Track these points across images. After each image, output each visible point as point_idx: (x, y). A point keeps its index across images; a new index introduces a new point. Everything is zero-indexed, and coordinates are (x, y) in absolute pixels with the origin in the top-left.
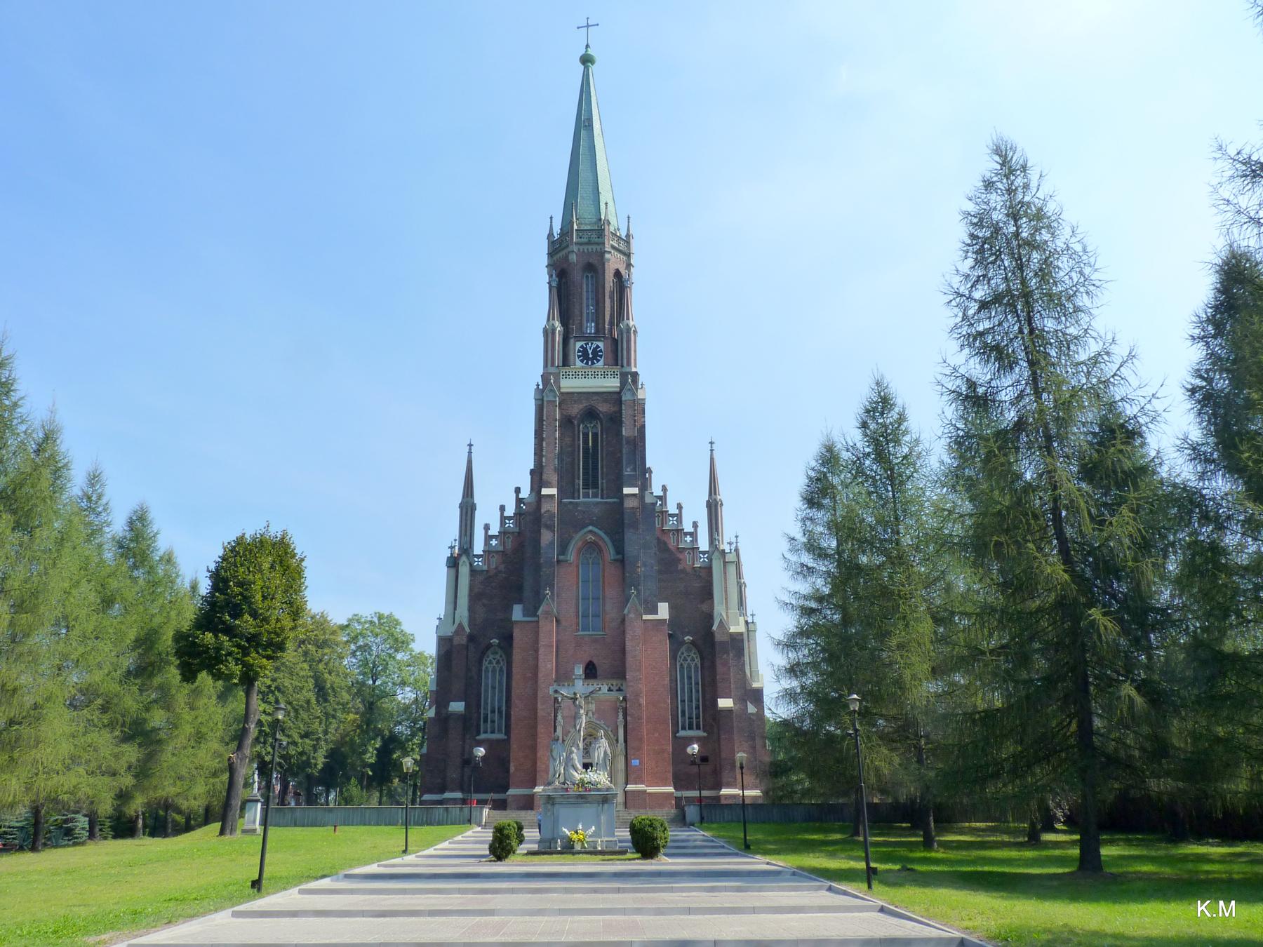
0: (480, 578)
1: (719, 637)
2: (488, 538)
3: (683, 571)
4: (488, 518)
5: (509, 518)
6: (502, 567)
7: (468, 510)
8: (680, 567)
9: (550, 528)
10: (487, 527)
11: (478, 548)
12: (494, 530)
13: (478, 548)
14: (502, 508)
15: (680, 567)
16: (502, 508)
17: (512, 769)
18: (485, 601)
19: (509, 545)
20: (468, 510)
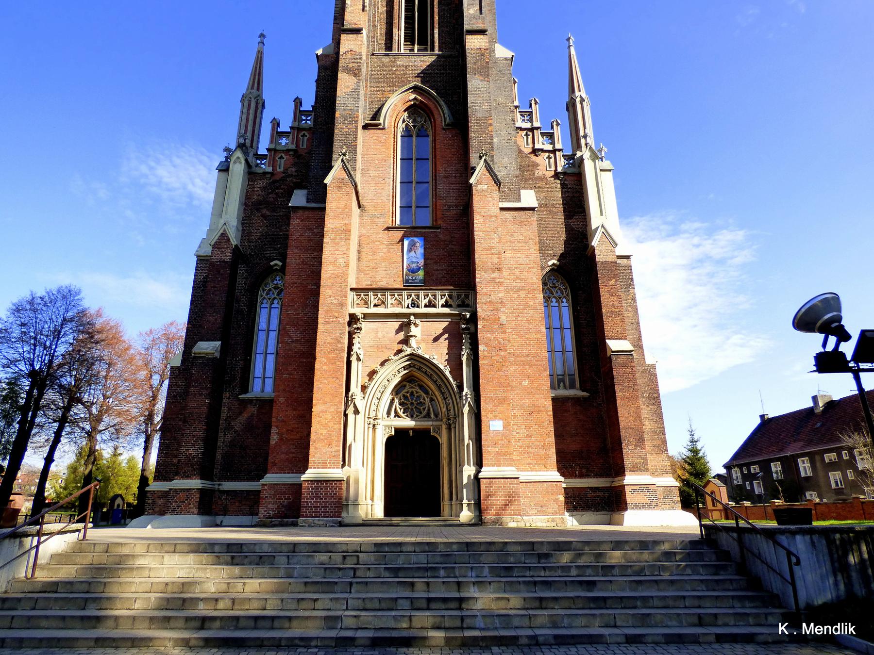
0: (261, 183)
1: (600, 257)
2: (277, 134)
3: (542, 178)
4: (279, 111)
5: (306, 113)
6: (292, 171)
7: (254, 105)
8: (538, 173)
9: (355, 73)
10: (276, 123)
11: (264, 145)
12: (285, 126)
13: (264, 145)
14: (298, 102)
15: (538, 173)
16: (298, 102)
17: (274, 439)
18: (265, 212)
19: (304, 144)
20: (254, 105)
